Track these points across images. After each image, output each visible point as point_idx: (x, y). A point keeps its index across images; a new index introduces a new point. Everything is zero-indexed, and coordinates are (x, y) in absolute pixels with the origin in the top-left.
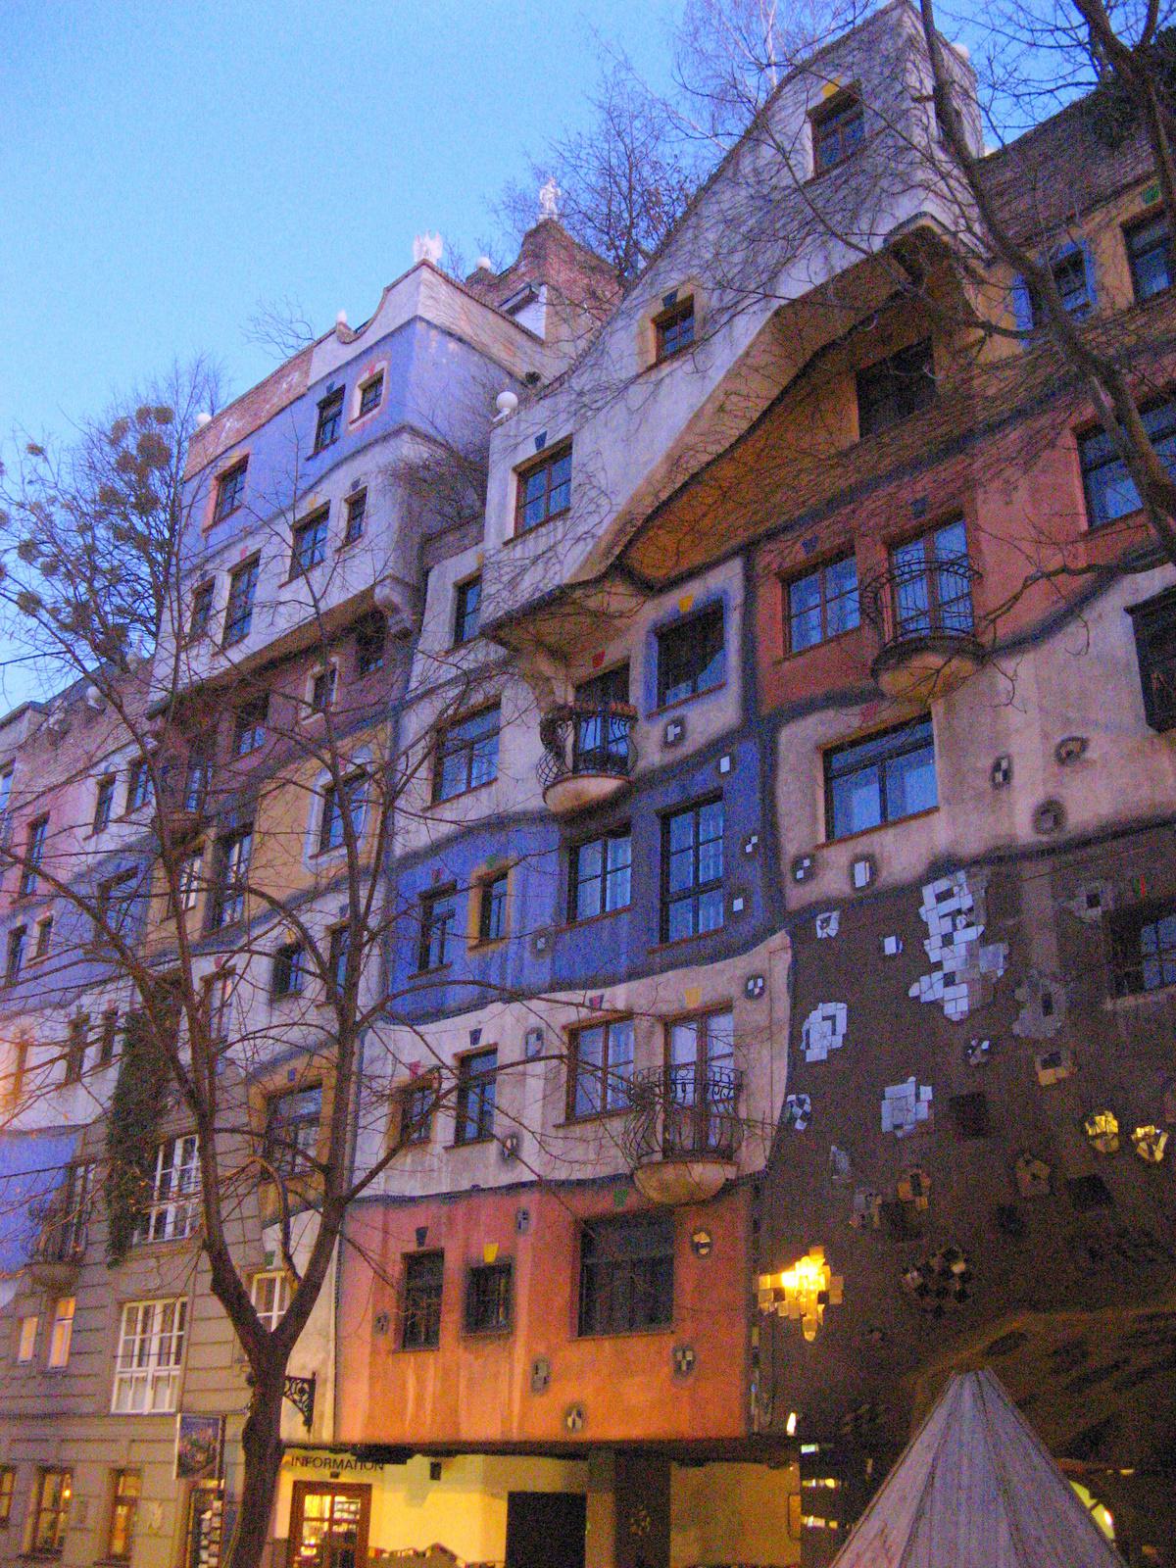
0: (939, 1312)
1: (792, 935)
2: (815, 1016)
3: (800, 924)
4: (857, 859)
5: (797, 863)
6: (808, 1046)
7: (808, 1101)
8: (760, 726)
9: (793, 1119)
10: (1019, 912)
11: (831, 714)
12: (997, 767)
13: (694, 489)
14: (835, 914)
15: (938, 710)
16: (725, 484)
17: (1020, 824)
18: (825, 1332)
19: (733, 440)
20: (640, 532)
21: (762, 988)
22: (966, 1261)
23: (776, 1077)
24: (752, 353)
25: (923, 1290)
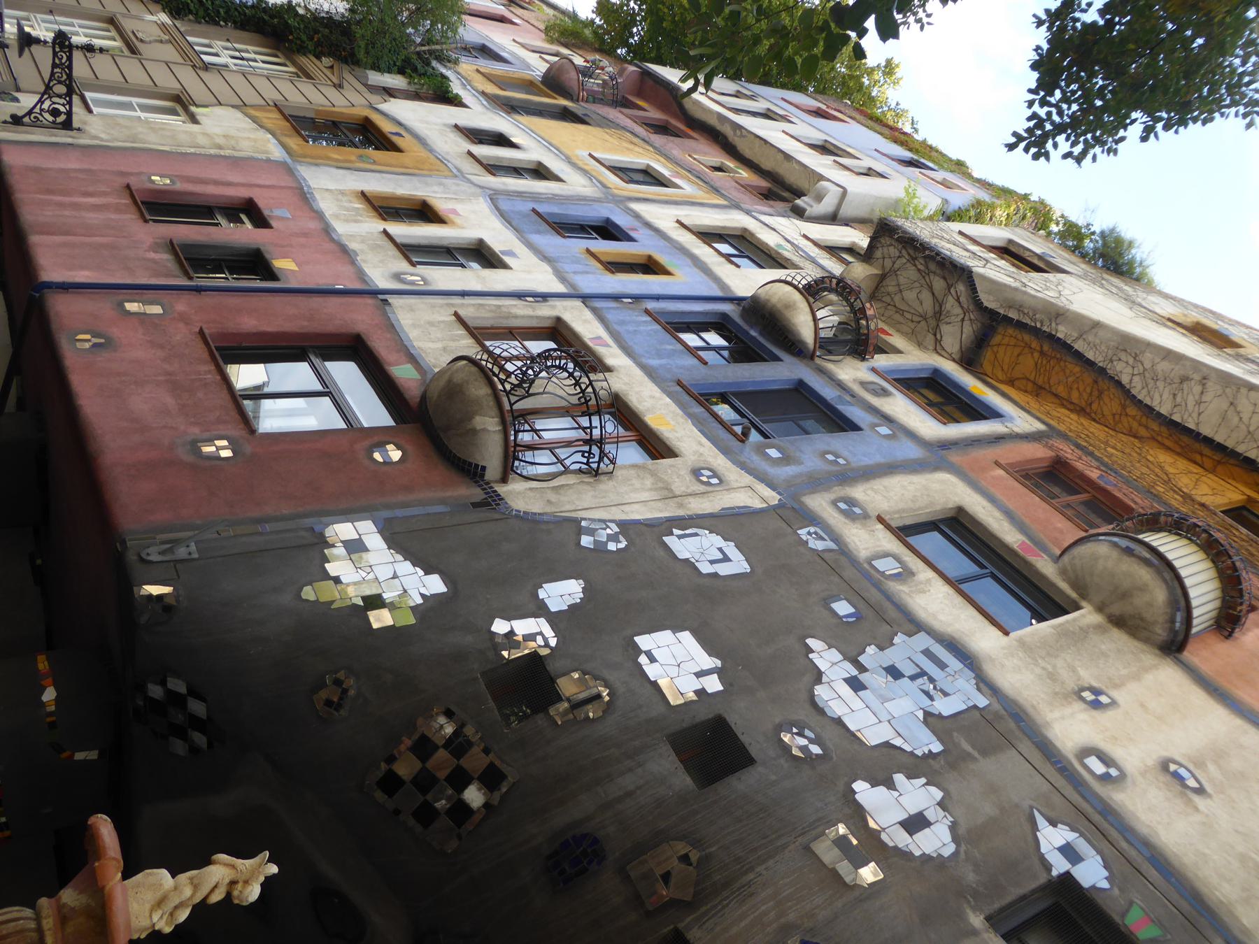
0: (391, 783)
1: (781, 505)
2: (718, 541)
3: (792, 512)
4: (897, 558)
5: (851, 502)
6: (680, 537)
7: (622, 545)
8: (938, 455)
9: (591, 532)
10: (985, 753)
11: (998, 514)
12: (1096, 692)
13: (1088, 378)
14: (830, 545)
15: (1086, 616)
16: (1094, 406)
17: (1070, 729)
18: (324, 608)
19: (1147, 401)
20: (1036, 332)
21: (708, 484)
22: (486, 805)
23: (626, 508)
24: (1253, 394)
25: (424, 747)
